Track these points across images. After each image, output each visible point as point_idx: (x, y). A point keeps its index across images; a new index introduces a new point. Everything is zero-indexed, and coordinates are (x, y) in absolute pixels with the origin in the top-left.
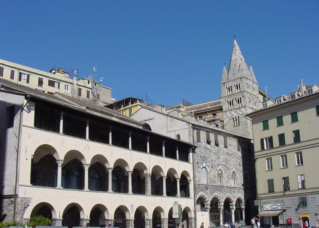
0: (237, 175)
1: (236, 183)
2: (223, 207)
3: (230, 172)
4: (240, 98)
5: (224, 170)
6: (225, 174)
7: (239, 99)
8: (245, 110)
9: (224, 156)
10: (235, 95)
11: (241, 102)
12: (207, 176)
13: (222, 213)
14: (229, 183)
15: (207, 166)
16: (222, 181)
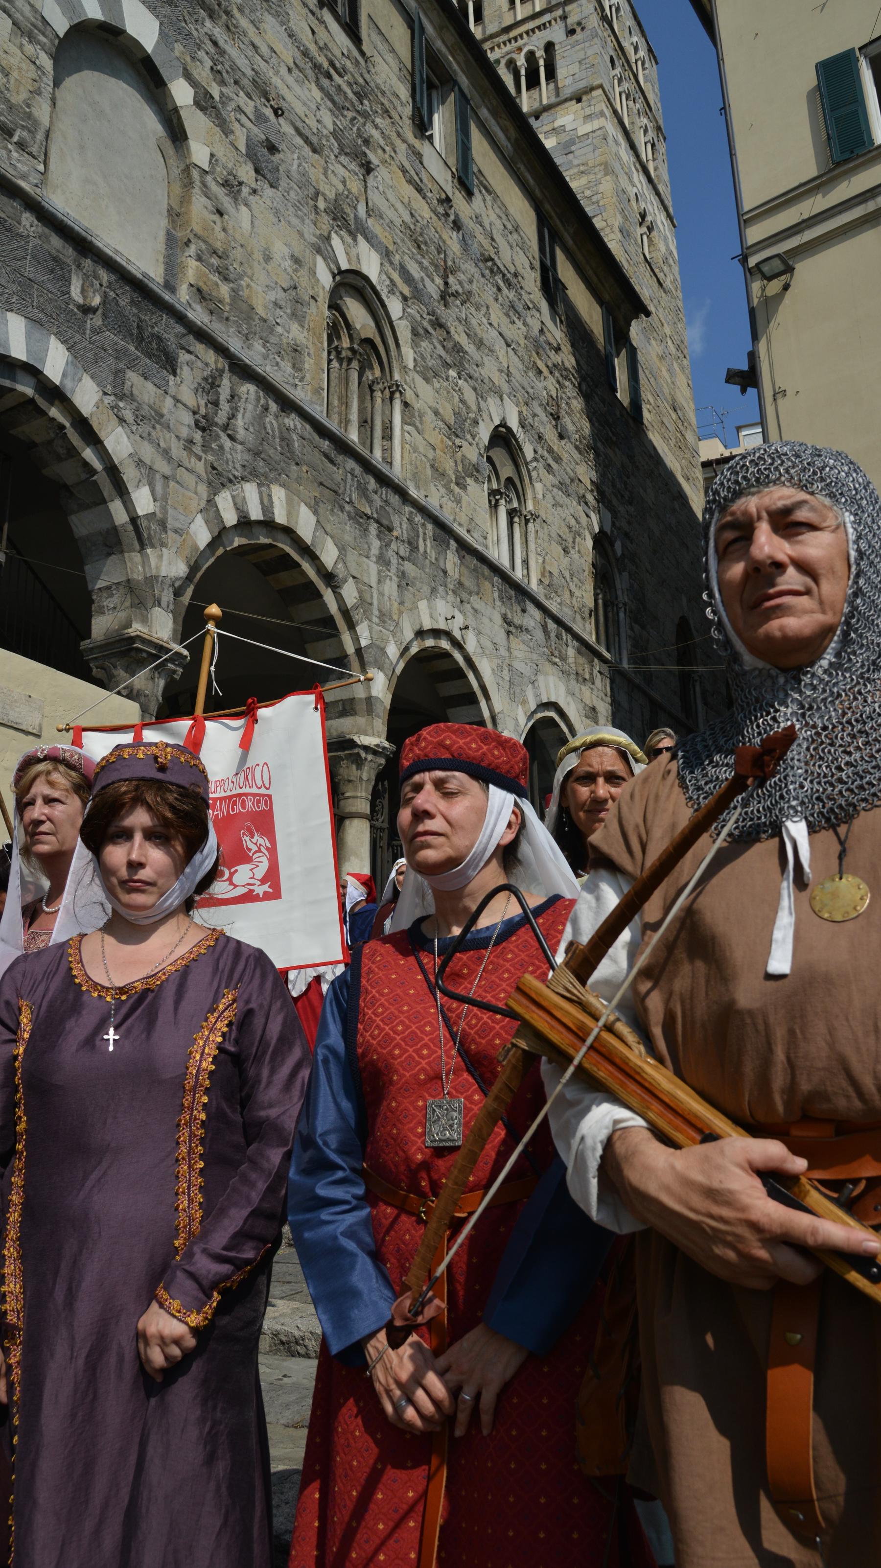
0: (538, 486)
1: (526, 562)
2: (380, 725)
3: (474, 407)
4: (549, 47)
5: (415, 333)
6: (427, 380)
7: (540, 54)
8: (588, 118)
9: (425, 212)
10: (504, 37)
11: (551, 74)
12: (175, 216)
13: (364, 807)
14: (458, 501)
15: (188, 76)
16: (388, 435)
